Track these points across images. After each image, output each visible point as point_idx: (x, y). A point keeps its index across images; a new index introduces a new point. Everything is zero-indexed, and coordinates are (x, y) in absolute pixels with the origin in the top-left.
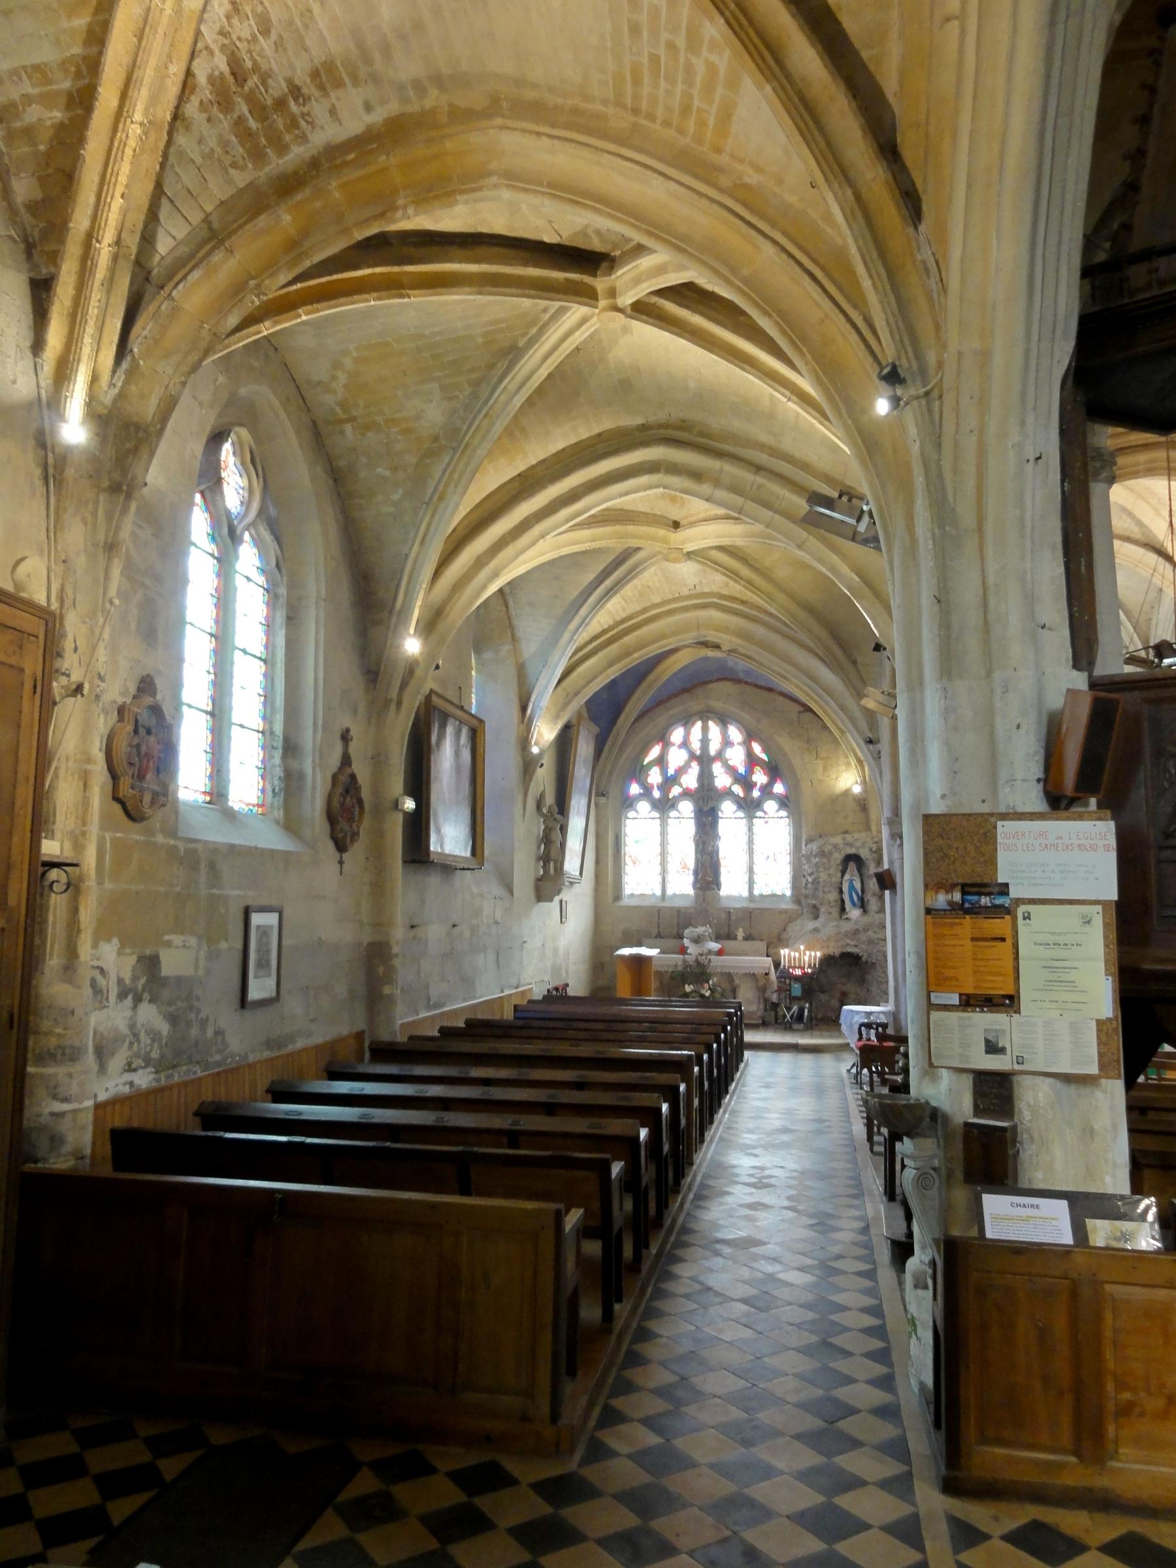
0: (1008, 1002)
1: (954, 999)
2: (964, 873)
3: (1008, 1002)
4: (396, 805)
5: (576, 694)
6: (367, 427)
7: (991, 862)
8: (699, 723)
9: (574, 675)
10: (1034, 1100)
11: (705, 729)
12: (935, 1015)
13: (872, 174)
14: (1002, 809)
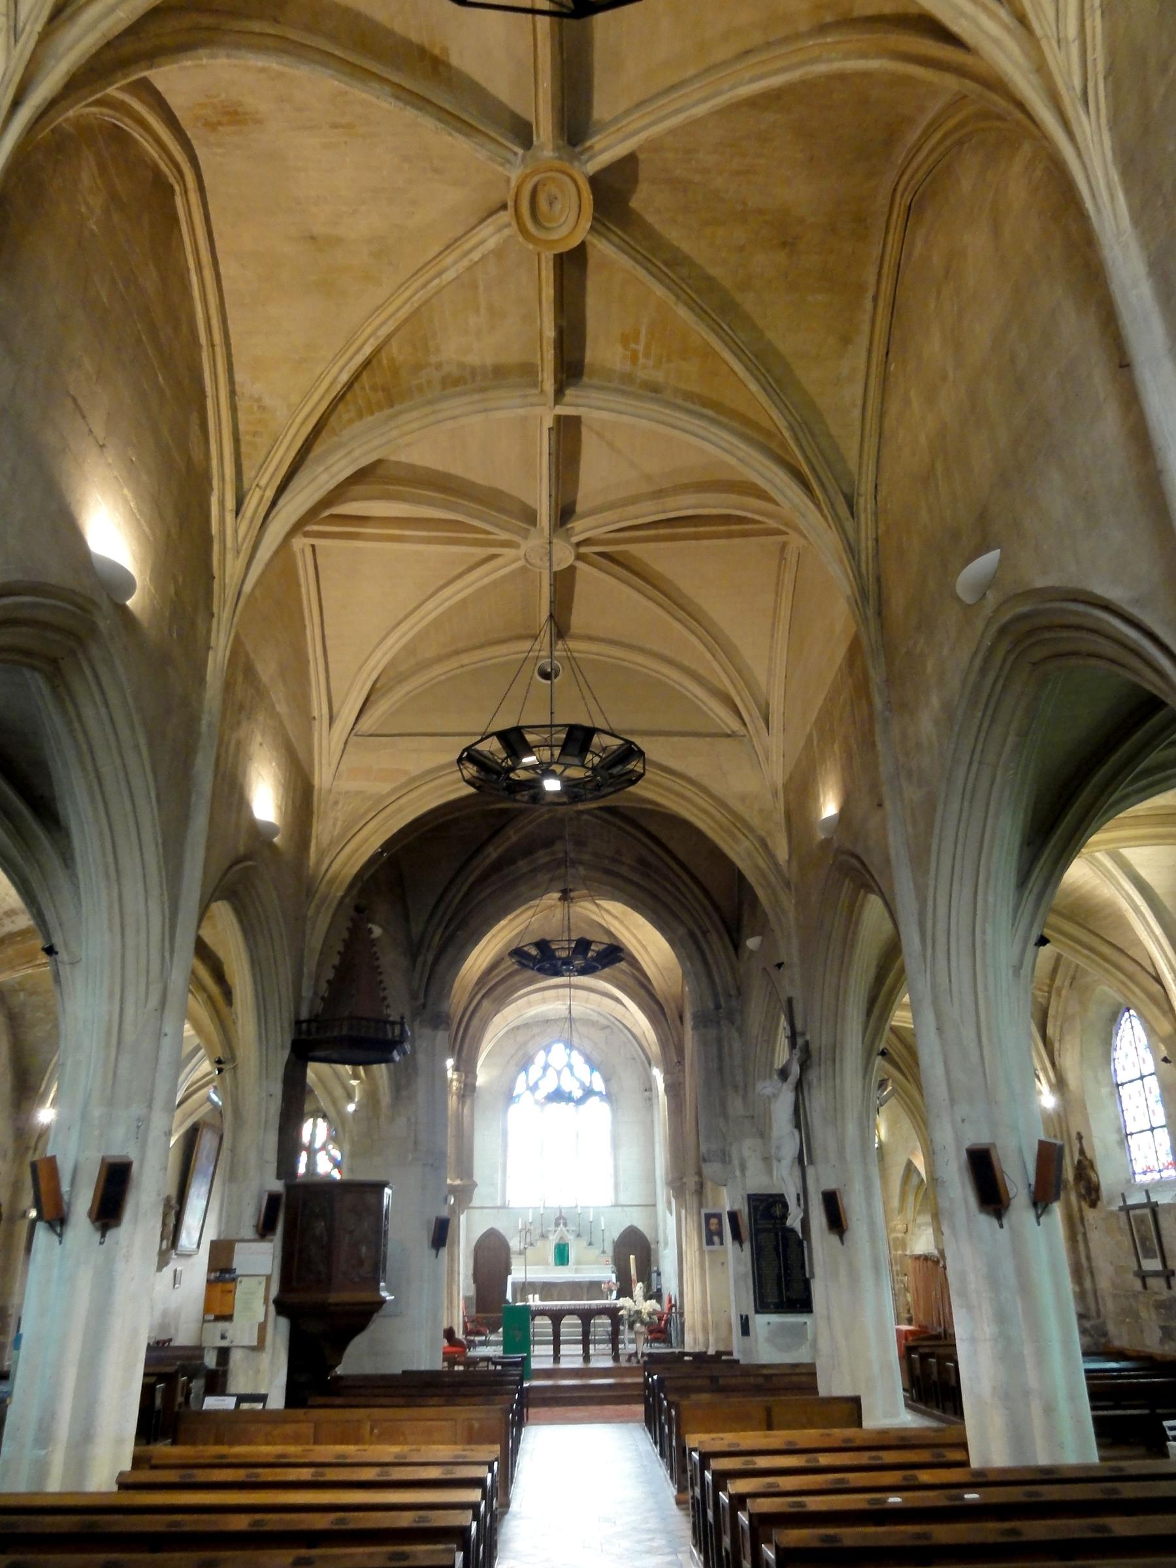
0: (228, 1318)
1: (212, 1317)
2: (222, 1265)
3: (228, 1318)
4: (24, 1214)
5: (191, 1115)
6: (31, 994)
7: (231, 1259)
8: (311, 1120)
9: (190, 1101)
10: (236, 1357)
11: (315, 1125)
12: (206, 1325)
13: (214, 989)
14: (240, 1237)
